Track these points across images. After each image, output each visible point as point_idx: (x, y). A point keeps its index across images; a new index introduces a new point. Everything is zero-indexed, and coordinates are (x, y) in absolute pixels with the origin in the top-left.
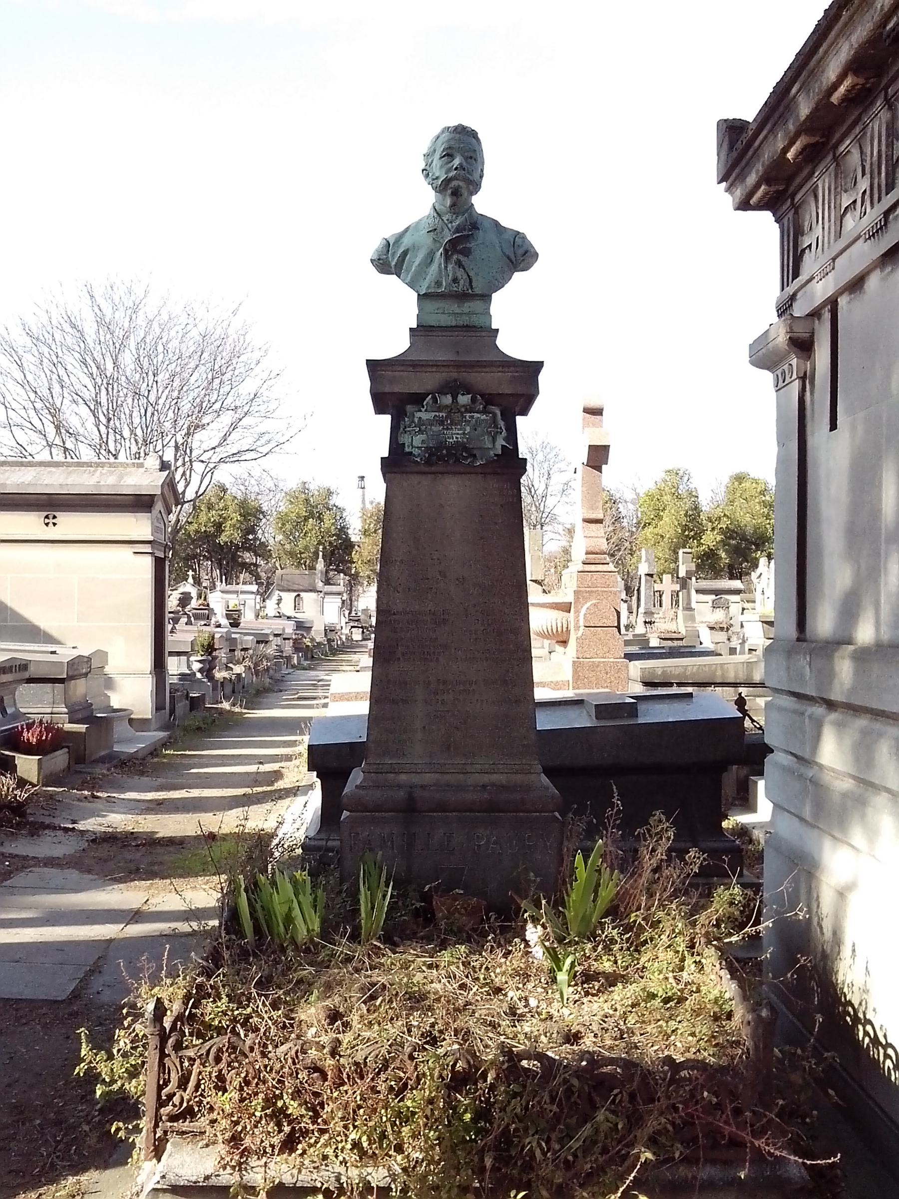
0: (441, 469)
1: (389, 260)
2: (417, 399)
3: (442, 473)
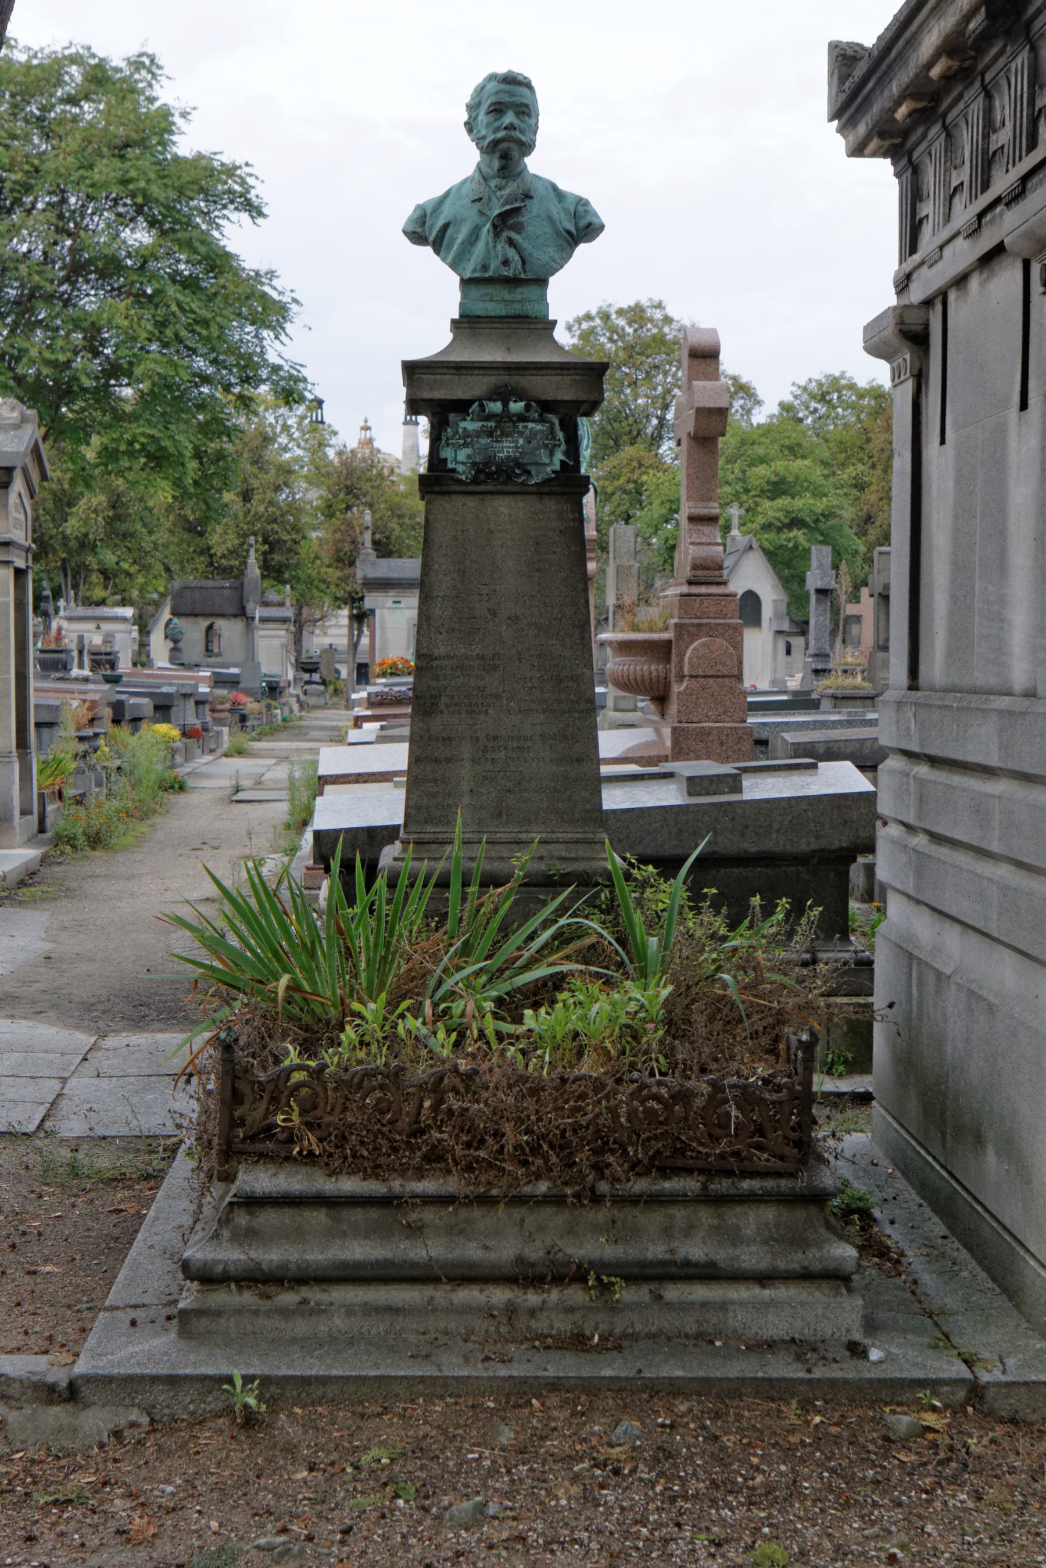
0: (490, 488)
1: (427, 230)
2: (462, 407)
3: (492, 493)
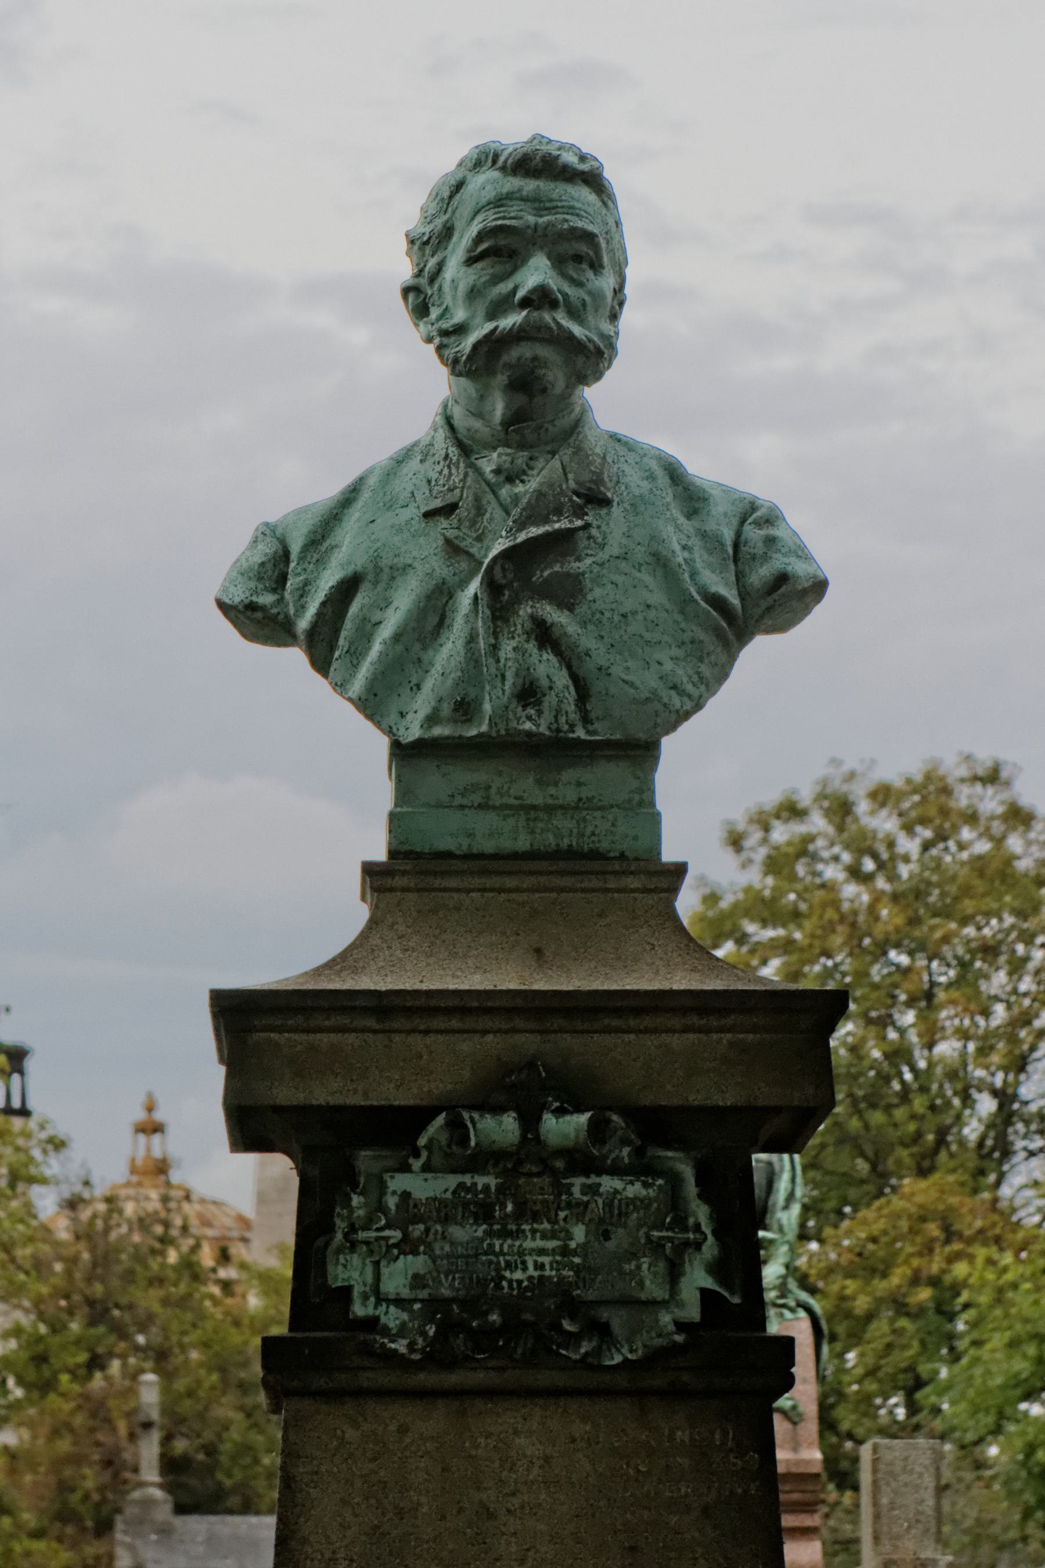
0: (478, 1378)
1: (286, 599)
2: (396, 1129)
3: (488, 1393)
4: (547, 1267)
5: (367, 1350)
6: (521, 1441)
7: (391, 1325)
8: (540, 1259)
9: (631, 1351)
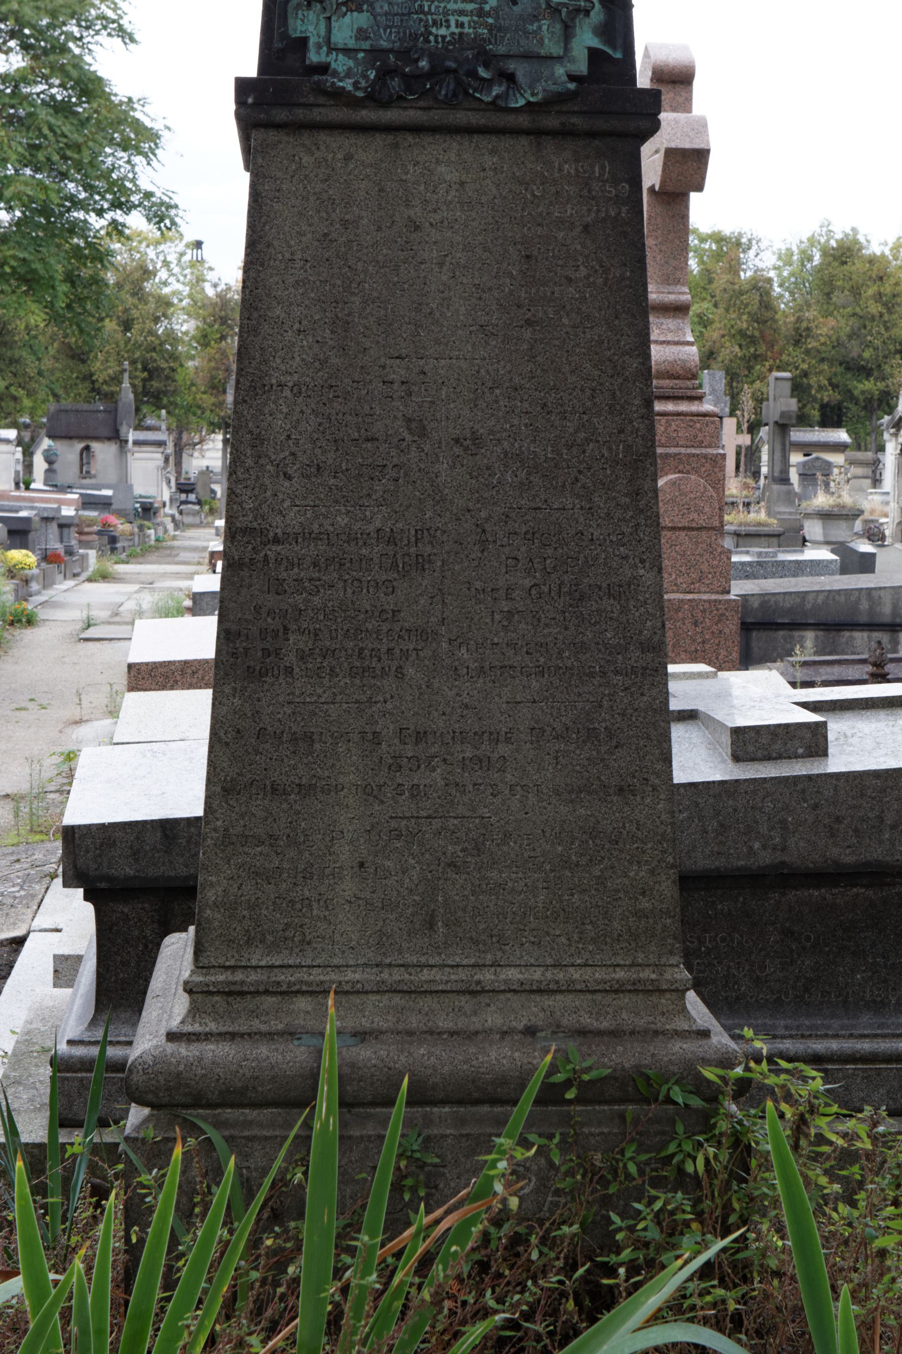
0: (411, 115)
3: (416, 129)
4: (466, 25)
5: (320, 90)
6: (442, 169)
7: (340, 69)
8: (461, 19)
9: (533, 95)
